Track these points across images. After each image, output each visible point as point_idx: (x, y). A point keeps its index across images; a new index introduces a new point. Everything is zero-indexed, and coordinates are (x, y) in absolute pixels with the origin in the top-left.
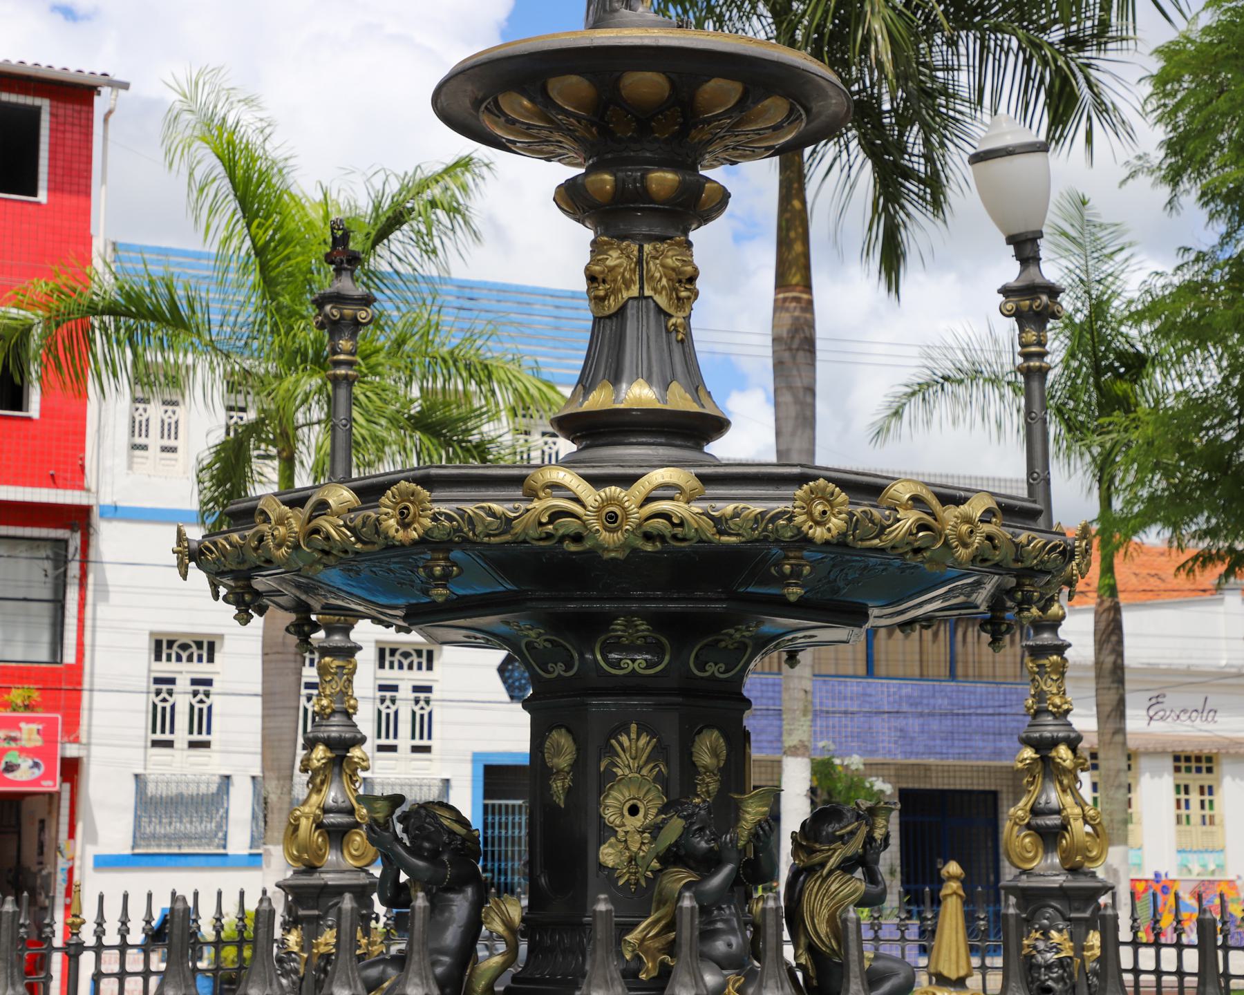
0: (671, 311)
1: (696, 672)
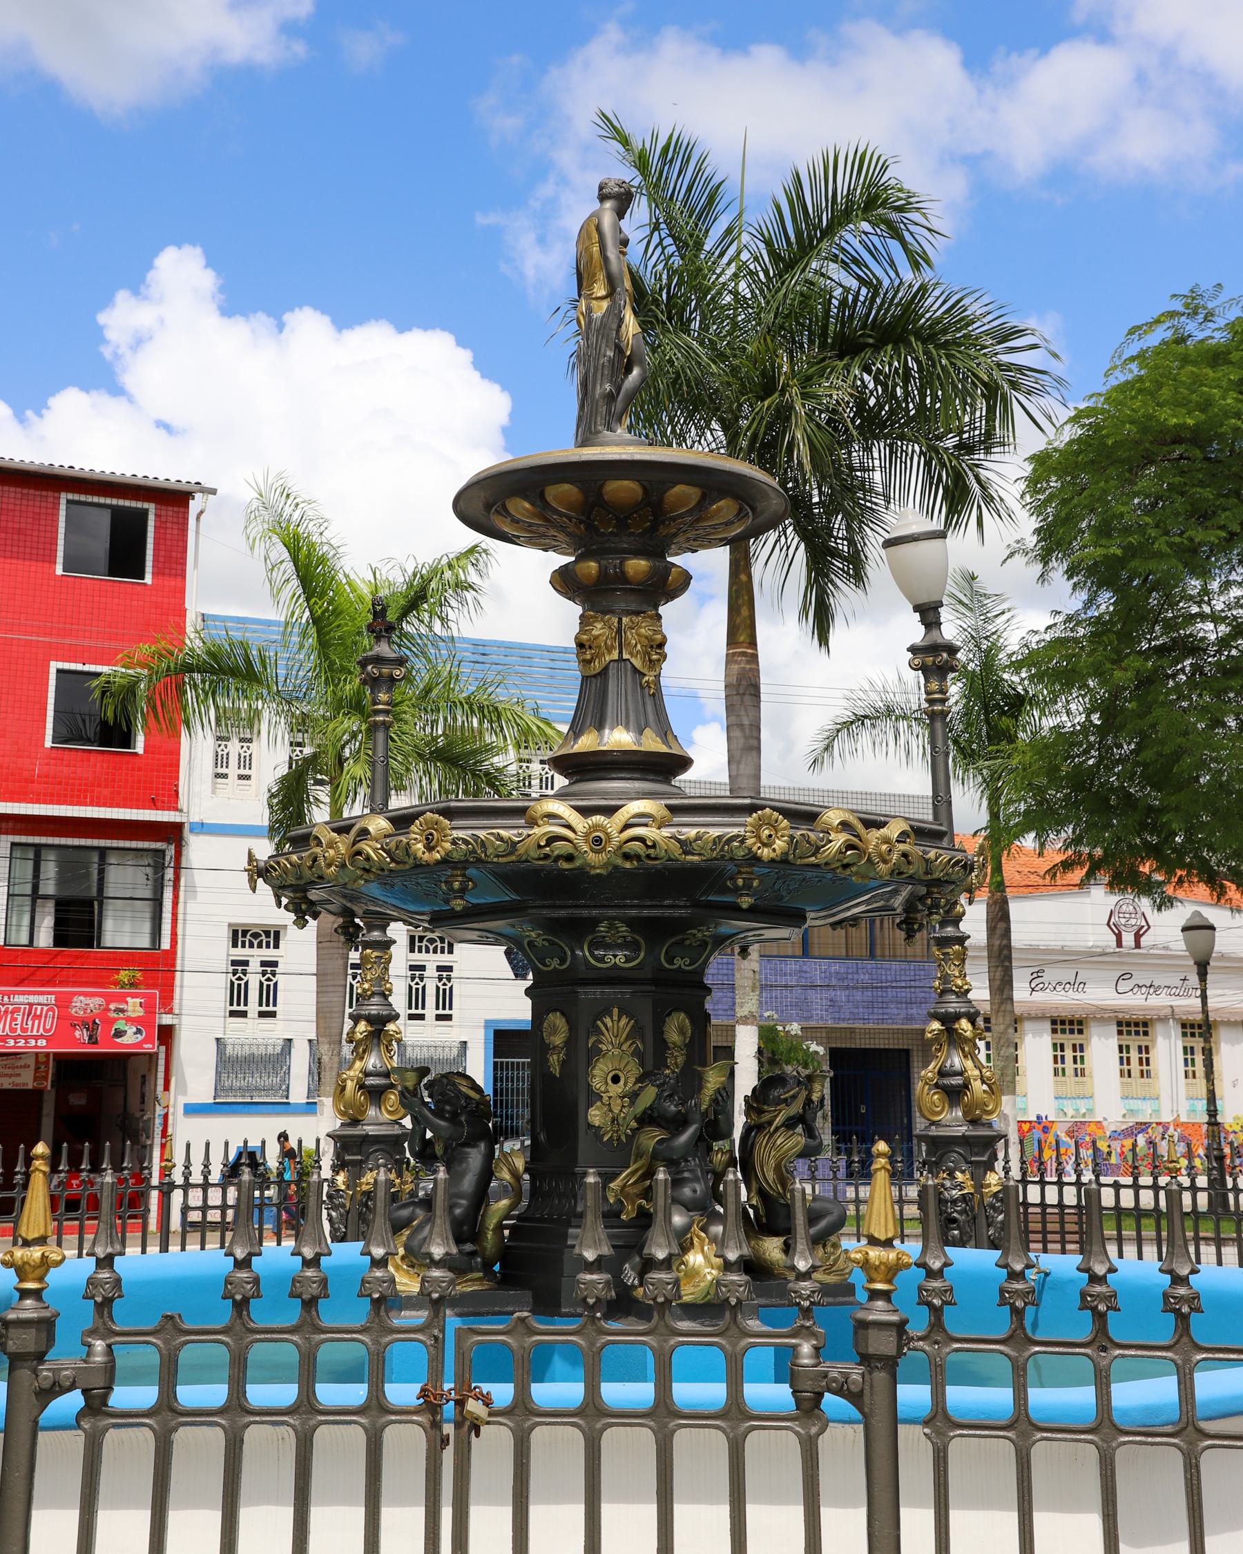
0: (645, 671)
1: (667, 966)
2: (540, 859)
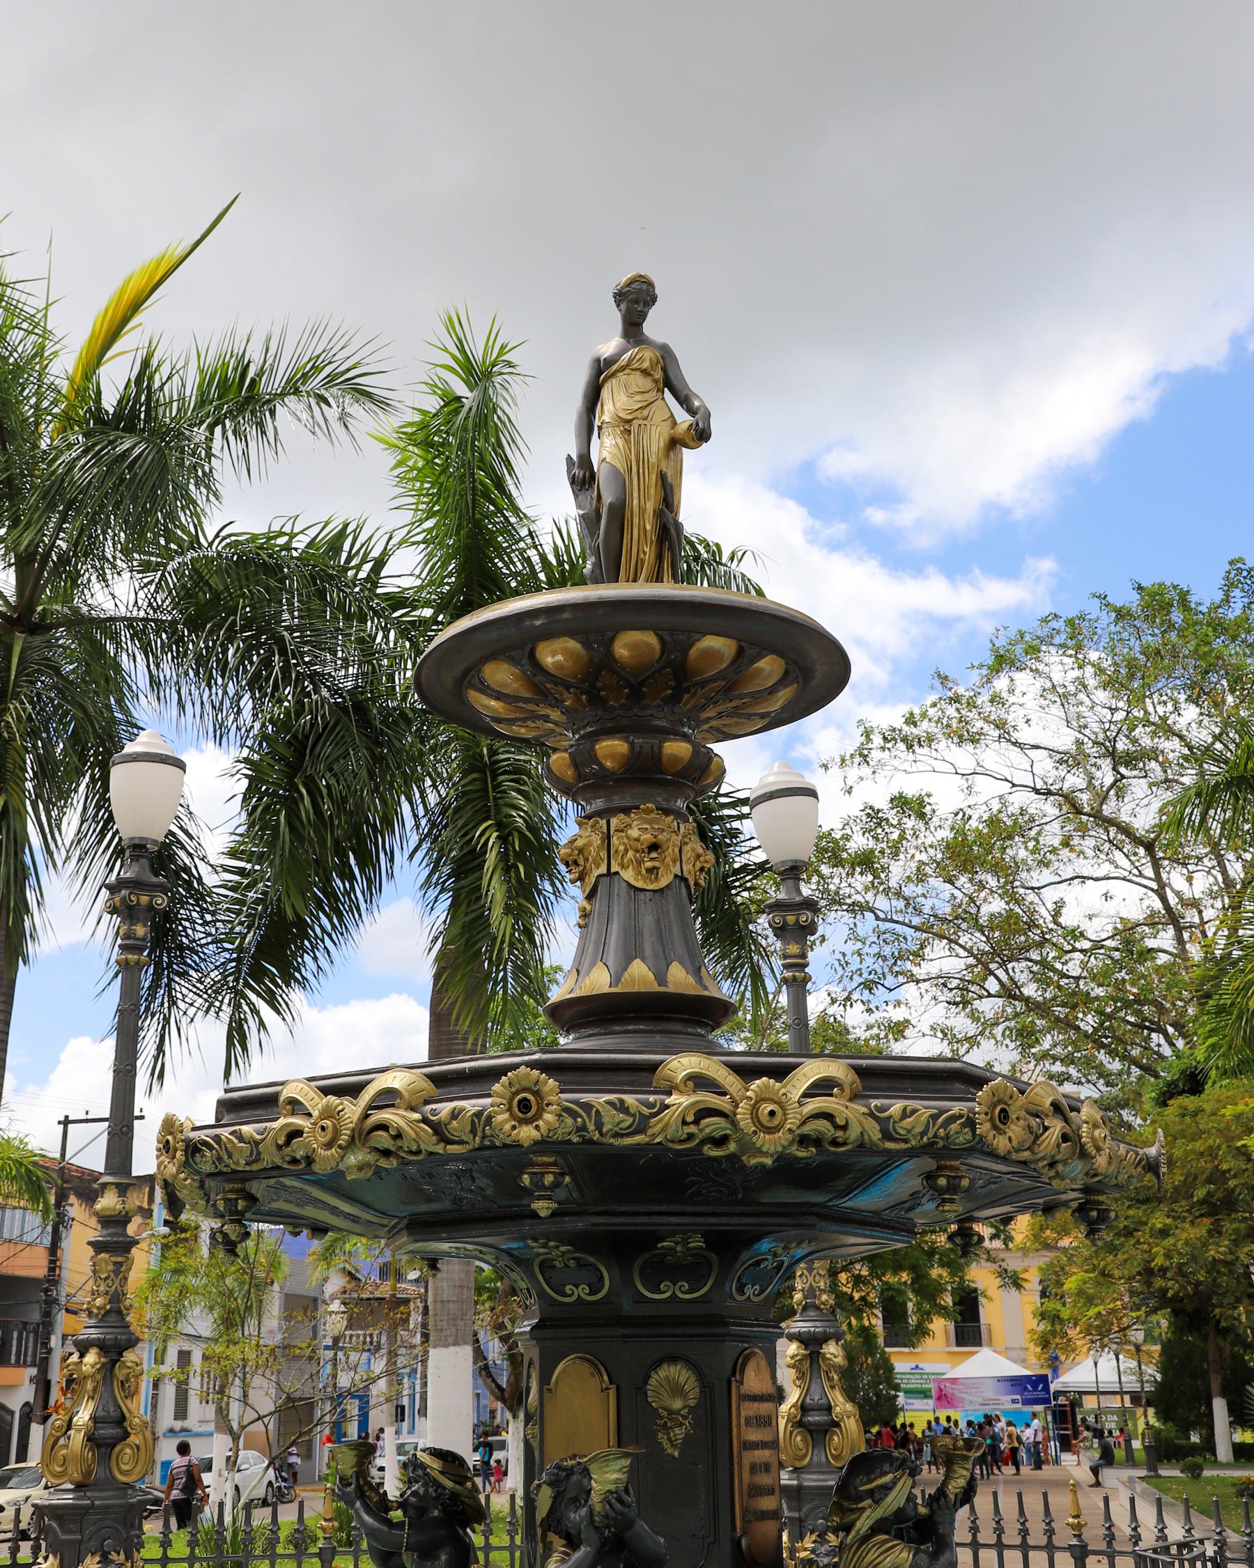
2: (681, 1141)
